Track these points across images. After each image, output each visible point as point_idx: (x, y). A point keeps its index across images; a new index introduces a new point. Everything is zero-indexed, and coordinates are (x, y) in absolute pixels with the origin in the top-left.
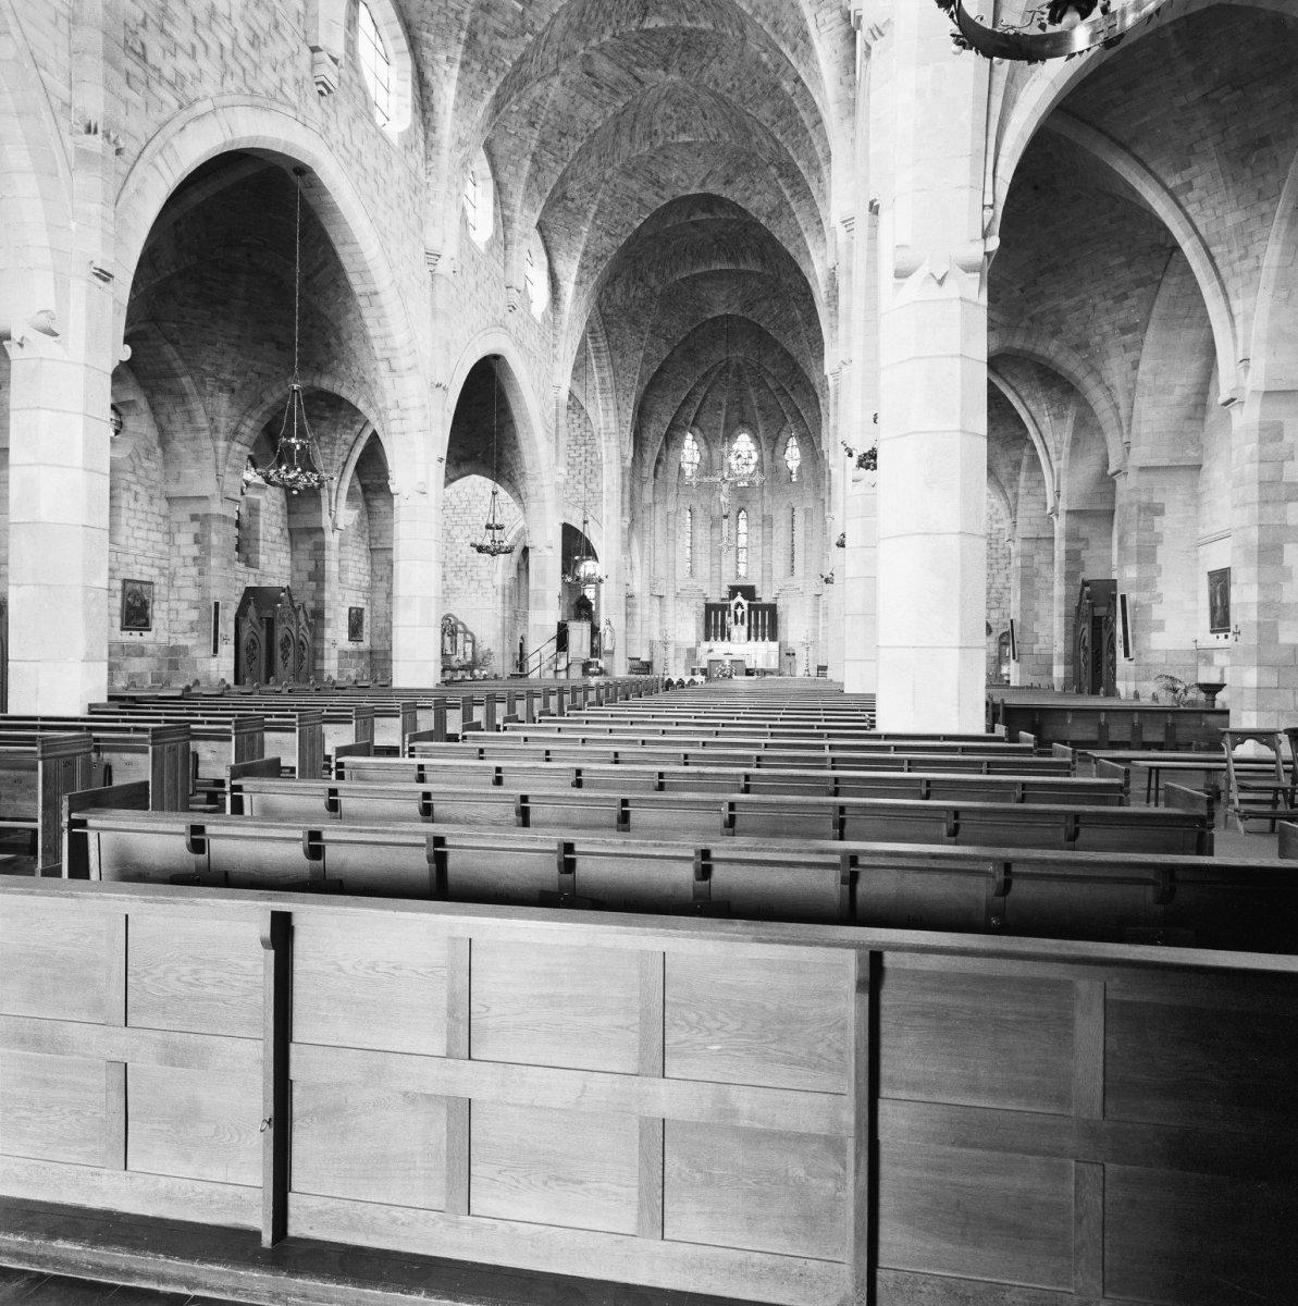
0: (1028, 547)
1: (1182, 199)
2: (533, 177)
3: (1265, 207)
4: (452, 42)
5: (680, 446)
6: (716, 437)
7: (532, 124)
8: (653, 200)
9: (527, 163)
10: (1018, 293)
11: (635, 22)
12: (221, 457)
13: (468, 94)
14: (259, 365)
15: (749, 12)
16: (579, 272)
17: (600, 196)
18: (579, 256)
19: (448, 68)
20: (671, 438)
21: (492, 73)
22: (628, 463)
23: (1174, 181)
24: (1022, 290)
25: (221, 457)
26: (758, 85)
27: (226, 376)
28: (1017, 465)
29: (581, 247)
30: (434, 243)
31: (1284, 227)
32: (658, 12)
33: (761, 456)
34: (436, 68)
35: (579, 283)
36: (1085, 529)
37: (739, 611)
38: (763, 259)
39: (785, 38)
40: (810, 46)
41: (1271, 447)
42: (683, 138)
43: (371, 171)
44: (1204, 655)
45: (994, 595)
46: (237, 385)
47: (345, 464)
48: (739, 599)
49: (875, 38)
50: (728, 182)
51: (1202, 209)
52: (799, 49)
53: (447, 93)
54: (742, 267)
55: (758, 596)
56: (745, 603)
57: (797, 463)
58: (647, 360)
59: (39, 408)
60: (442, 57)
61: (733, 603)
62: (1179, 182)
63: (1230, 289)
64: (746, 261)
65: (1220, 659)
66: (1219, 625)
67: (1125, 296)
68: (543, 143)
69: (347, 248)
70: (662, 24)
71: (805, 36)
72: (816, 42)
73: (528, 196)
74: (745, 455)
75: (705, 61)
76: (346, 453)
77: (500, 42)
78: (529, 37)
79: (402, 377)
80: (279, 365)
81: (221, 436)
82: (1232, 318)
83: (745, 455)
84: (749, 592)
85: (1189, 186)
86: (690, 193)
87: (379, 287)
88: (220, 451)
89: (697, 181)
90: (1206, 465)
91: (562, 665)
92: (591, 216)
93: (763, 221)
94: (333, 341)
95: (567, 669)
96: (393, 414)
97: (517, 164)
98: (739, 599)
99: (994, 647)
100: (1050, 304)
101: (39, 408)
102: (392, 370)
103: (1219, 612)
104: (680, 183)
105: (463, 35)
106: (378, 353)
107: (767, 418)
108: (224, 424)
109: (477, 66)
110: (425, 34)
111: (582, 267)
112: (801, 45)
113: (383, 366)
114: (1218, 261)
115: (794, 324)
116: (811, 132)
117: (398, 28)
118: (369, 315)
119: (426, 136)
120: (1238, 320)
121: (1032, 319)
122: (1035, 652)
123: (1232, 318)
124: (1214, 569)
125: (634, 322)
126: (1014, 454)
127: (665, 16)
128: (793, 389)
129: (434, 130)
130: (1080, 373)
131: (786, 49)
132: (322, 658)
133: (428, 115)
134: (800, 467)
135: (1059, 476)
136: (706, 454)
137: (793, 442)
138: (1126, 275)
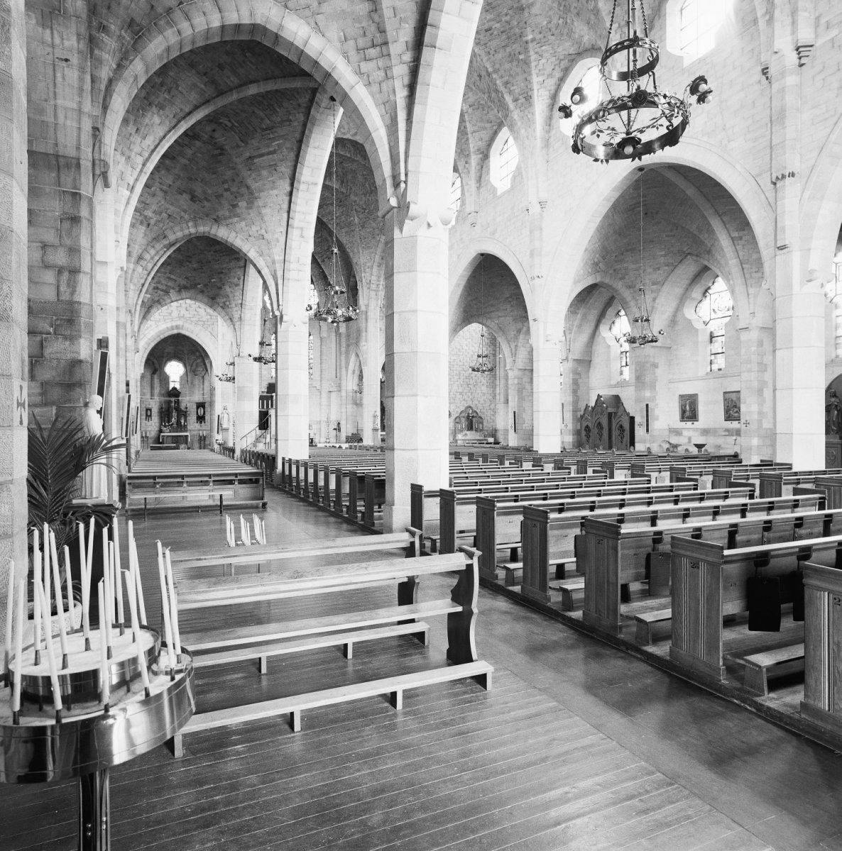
0: (520, 373)
14: (172, 209)
15: (490, 70)
23: (735, 234)
27: (149, 213)
28: (519, 331)
38: (342, 182)
39: (510, 92)
40: (531, 105)
44: (677, 432)
46: (152, 222)
49: (789, 176)
51: (743, 248)
59: (438, 273)
62: (737, 235)
63: (748, 282)
65: (685, 433)
66: (687, 418)
67: (659, 269)
69: (316, 152)
71: (528, 98)
76: (145, 277)
79: (307, 242)
80: (185, 211)
82: (748, 295)
85: (741, 238)
89: (353, 131)
90: (675, 347)
94: (243, 204)
99: (452, 424)
100: (625, 265)
101: (438, 273)
102: (302, 236)
108: (136, 251)
114: (745, 271)
115: (350, 224)
116: (470, 135)
121: (615, 270)
122: (524, 428)
123: (748, 295)
124: (681, 394)
126: (519, 325)
130: (629, 299)
131: (508, 99)
135: (570, 341)
138: (662, 260)
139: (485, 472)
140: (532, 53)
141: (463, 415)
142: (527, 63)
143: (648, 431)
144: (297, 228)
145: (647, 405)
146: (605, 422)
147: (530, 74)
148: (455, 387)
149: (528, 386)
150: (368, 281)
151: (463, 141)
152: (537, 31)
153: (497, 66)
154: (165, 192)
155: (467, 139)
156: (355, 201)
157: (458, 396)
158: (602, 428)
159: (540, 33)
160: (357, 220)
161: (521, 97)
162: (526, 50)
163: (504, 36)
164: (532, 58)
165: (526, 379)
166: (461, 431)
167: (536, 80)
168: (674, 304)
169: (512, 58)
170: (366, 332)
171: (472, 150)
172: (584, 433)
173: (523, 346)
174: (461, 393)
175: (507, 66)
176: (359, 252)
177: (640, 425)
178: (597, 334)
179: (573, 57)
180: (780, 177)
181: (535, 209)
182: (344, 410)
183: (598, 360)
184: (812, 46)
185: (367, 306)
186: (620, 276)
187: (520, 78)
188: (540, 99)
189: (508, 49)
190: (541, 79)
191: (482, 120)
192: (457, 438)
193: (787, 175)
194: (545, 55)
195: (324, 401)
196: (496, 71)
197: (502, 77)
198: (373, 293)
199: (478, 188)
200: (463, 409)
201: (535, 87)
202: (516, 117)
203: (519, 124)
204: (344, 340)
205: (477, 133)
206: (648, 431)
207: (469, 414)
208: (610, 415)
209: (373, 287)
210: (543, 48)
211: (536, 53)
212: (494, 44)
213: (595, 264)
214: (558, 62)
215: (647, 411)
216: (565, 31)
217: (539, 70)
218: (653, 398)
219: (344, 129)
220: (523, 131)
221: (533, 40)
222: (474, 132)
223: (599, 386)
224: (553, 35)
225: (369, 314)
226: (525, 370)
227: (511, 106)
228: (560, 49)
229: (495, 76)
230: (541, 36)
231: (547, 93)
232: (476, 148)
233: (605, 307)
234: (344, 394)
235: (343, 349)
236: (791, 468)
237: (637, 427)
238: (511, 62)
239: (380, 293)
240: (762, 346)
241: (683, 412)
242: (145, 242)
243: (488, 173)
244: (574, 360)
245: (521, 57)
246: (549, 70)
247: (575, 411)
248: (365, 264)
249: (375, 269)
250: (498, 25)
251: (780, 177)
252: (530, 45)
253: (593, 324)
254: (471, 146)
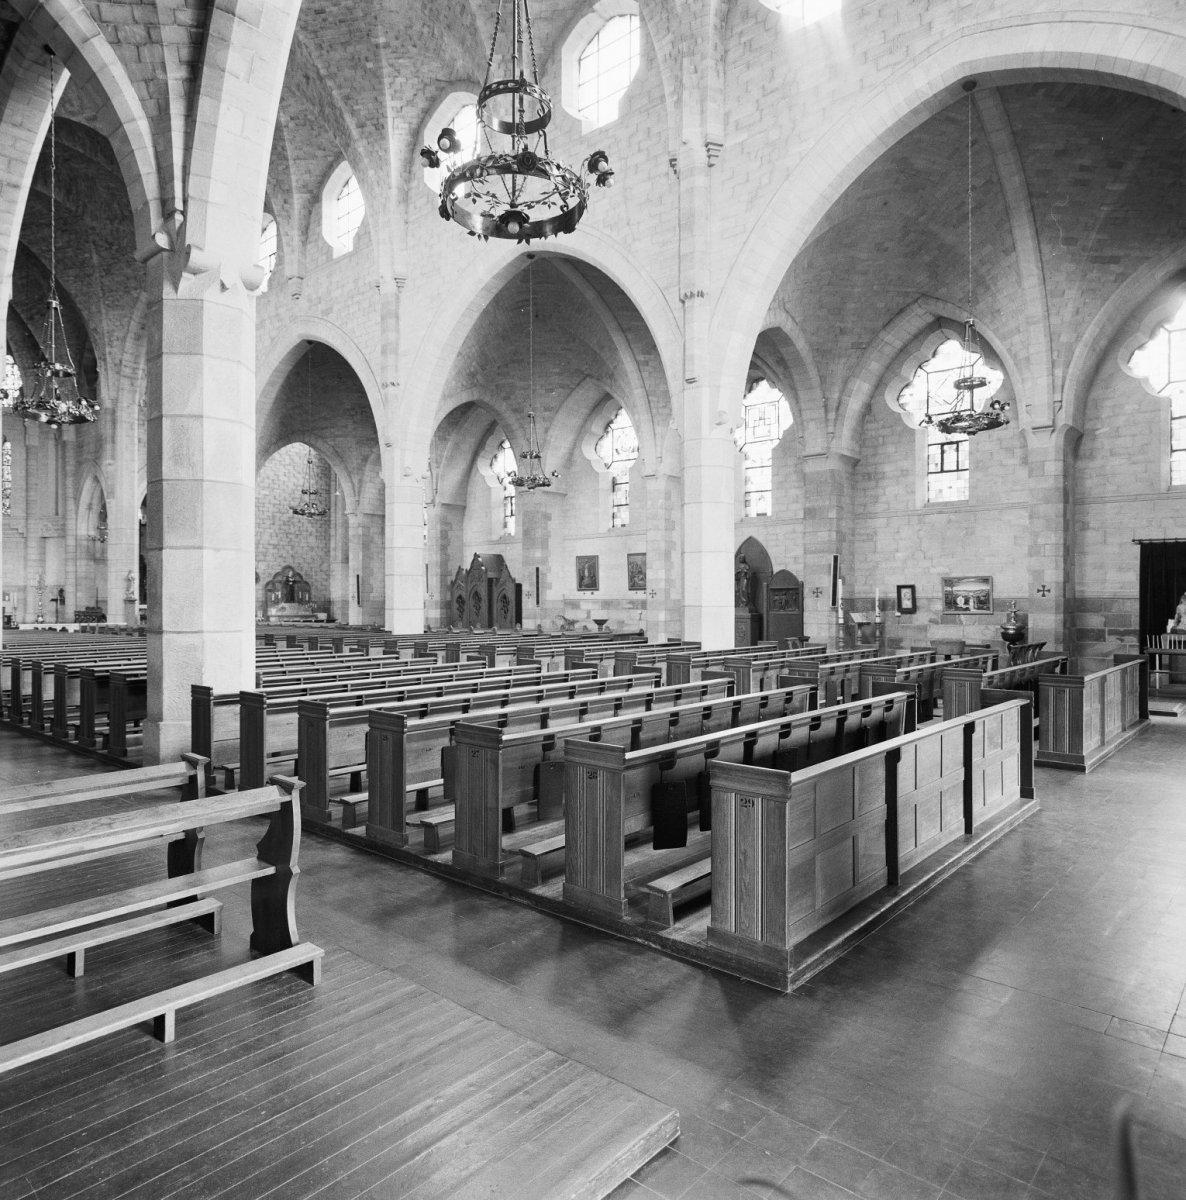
0: (367, 520)
1: (641, 367)
10: (495, 369)
15: (323, 72)
23: (641, 358)
24: (499, 368)
28: (365, 459)
36: (450, 518)
39: (353, 113)
44: (574, 605)
45: (261, 549)
52: (367, 129)
65: (584, 606)
67: (552, 390)
71: (380, 127)
85: (647, 363)
86: (74, 119)
89: (88, 113)
90: (570, 494)
103: (586, 581)
104: (67, 106)
112: (370, 128)
114: (652, 404)
115: (83, 264)
116: (291, 162)
122: (371, 599)
126: (365, 450)
130: (515, 426)
131: (350, 122)
138: (556, 379)
139: (313, 663)
140: (384, 63)
141: (280, 578)
142: (376, 75)
143: (538, 603)
145: (537, 569)
146: (484, 593)
148: (266, 537)
149: (377, 539)
150: (117, 361)
151: (280, 168)
152: (392, 35)
153: (333, 69)
155: (287, 167)
156: (93, 228)
157: (272, 551)
158: (480, 599)
159: (397, 38)
160: (95, 259)
161: (368, 123)
162: (377, 59)
163: (344, 28)
164: (386, 71)
165: (374, 530)
166: (276, 602)
167: (390, 104)
168: (571, 438)
169: (356, 63)
170: (113, 442)
171: (294, 184)
172: (455, 605)
173: (370, 481)
174: (275, 546)
175: (348, 73)
176: (100, 312)
177: (529, 595)
178: (474, 470)
179: (443, 85)
180: (689, 294)
181: (389, 287)
182: (71, 568)
183: (475, 505)
184: (721, 145)
185: (115, 401)
186: (503, 394)
188: (397, 132)
189: (350, 49)
190: (398, 104)
191: (310, 144)
192: (269, 613)
193: (696, 293)
195: (33, 554)
196: (332, 76)
197: (340, 87)
198: (125, 383)
199: (304, 243)
200: (278, 569)
201: (390, 114)
202: (361, 149)
203: (366, 160)
204: (70, 453)
205: (303, 162)
206: (538, 603)
207: (288, 577)
208: (490, 581)
209: (127, 371)
210: (401, 61)
211: (391, 65)
212: (328, 35)
213: (472, 375)
214: (421, 86)
215: (538, 577)
216: (432, 46)
217: (395, 91)
218: (545, 561)
219: (72, 105)
220: (371, 173)
221: (387, 46)
222: (298, 159)
223: (475, 544)
224: (415, 46)
225: (118, 414)
226: (373, 515)
227: (355, 133)
228: (425, 69)
229: (330, 83)
231: (407, 126)
232: (301, 183)
233: (484, 436)
234: (71, 542)
235: (70, 468)
236: (699, 648)
237: (524, 599)
238: (354, 68)
239: (139, 382)
240: (669, 498)
241: (581, 578)
243: (319, 224)
244: (443, 504)
245: (370, 65)
246: (409, 94)
247: (444, 576)
248: (111, 333)
249: (129, 344)
250: (335, 9)
251: (689, 294)
252: (382, 52)
253: (469, 457)
254: (293, 178)
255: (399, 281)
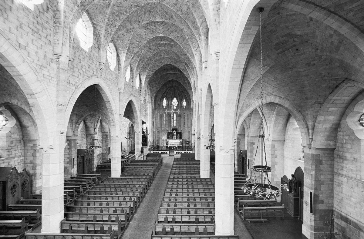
2: (138, 66)
3: (272, 111)
4: (125, 50)
5: (163, 101)
6: (170, 100)
7: (138, 57)
8: (160, 65)
9: (137, 64)
11: (160, 42)
12: (74, 128)
13: (127, 58)
16: (146, 78)
17: (150, 65)
18: (146, 76)
19: (123, 54)
20: (161, 100)
21: (132, 54)
22: (153, 108)
25: (74, 128)
26: (182, 53)
29: (146, 74)
30: (120, 87)
31: (275, 116)
32: (164, 41)
33: (178, 103)
34: (121, 54)
35: (145, 81)
36: (240, 137)
37: (174, 134)
39: (189, 54)
41: (273, 149)
42: (167, 56)
43: (109, 79)
47: (98, 120)
48: (174, 131)
50: (175, 63)
53: (123, 58)
54: (176, 73)
55: (178, 130)
56: (176, 132)
57: (186, 105)
58: (157, 88)
60: (122, 52)
61: (173, 132)
64: (177, 72)
68: (140, 60)
70: (164, 42)
71: (193, 55)
72: (195, 56)
73: (137, 69)
74: (175, 102)
75: (172, 47)
77: (134, 49)
78: (140, 47)
81: (74, 124)
83: (175, 102)
84: (176, 130)
87: (110, 100)
88: (74, 126)
91: (142, 156)
92: (148, 69)
93: (182, 71)
95: (143, 157)
96: (112, 122)
97: (135, 64)
98: (174, 131)
105: (127, 49)
106: (109, 111)
107: (179, 96)
109: (129, 53)
110: (119, 48)
111: (146, 78)
112: (192, 56)
113: (110, 113)
117: (114, 48)
118: (107, 105)
119: (119, 66)
120: (268, 127)
125: (155, 81)
127: (165, 41)
128: (185, 92)
129: (120, 65)
132: (93, 160)
133: (119, 62)
134: (186, 106)
136: (168, 102)
137: (184, 100)
140: (189, 42)
144: (110, 112)
147: (191, 48)
154: (78, 107)
160: (187, 82)
164: (190, 43)
175: (186, 46)
185: (193, 107)
187: (189, 49)
190: (195, 49)
194: (194, 42)
196: (184, 48)
197: (186, 49)
201: (194, 52)
212: (180, 40)
221: (189, 38)
230: (191, 37)
238: (186, 45)
242: (77, 118)
245: (188, 43)
255: (201, 89)
